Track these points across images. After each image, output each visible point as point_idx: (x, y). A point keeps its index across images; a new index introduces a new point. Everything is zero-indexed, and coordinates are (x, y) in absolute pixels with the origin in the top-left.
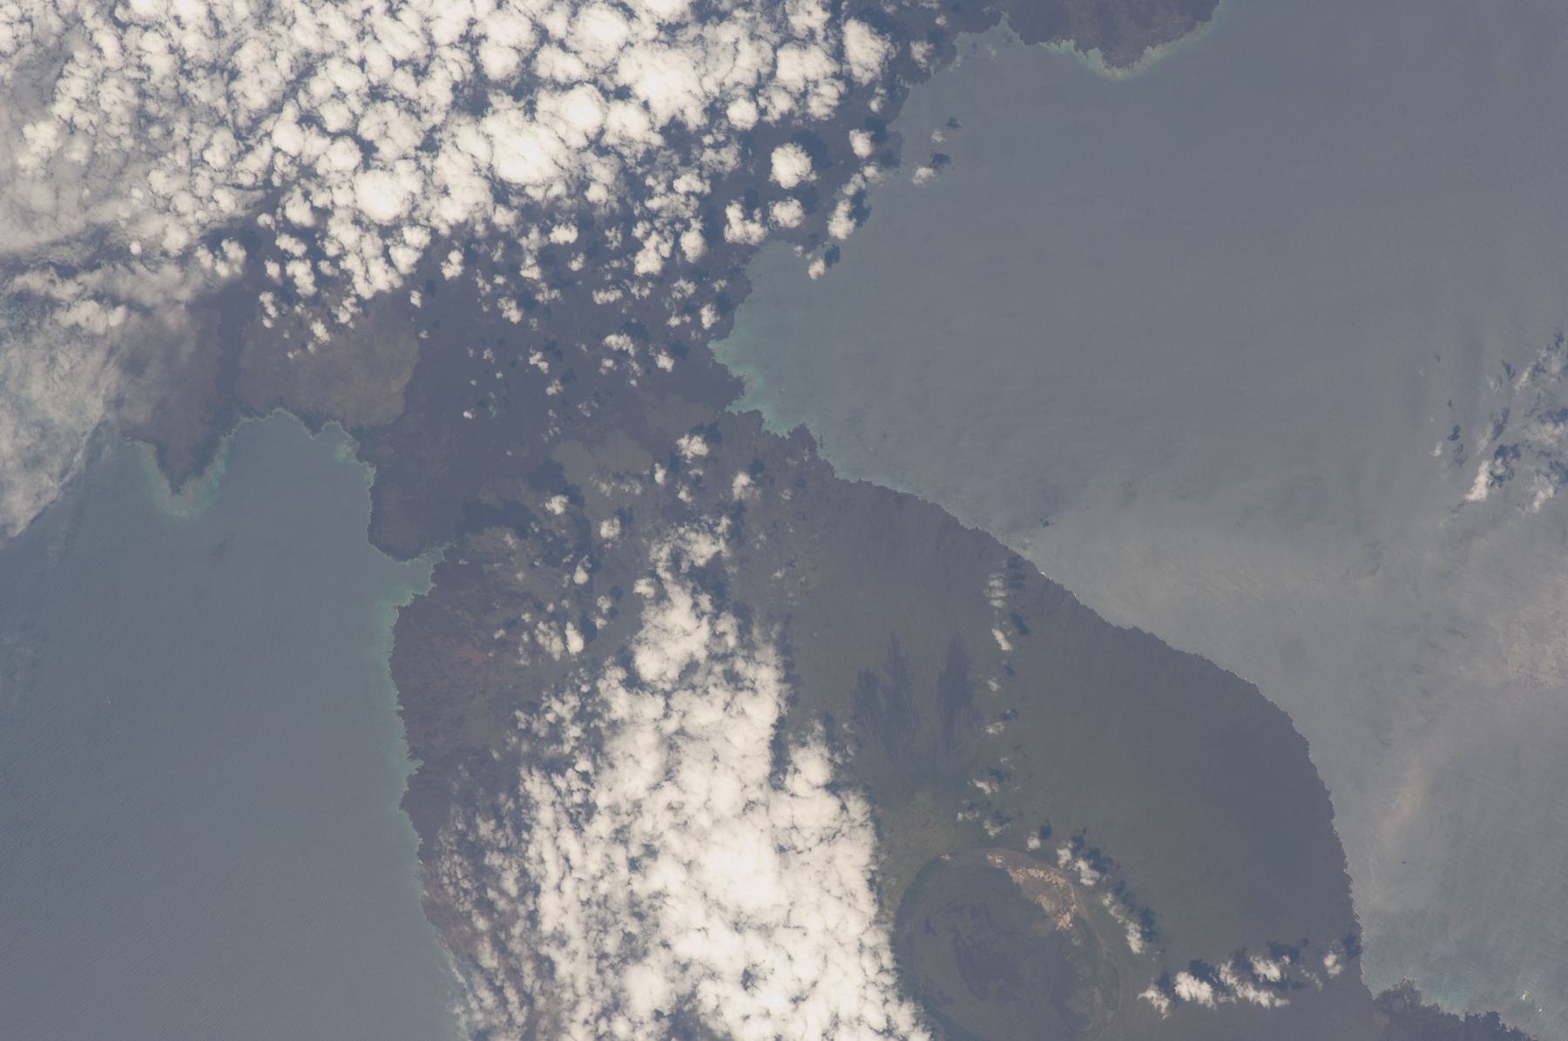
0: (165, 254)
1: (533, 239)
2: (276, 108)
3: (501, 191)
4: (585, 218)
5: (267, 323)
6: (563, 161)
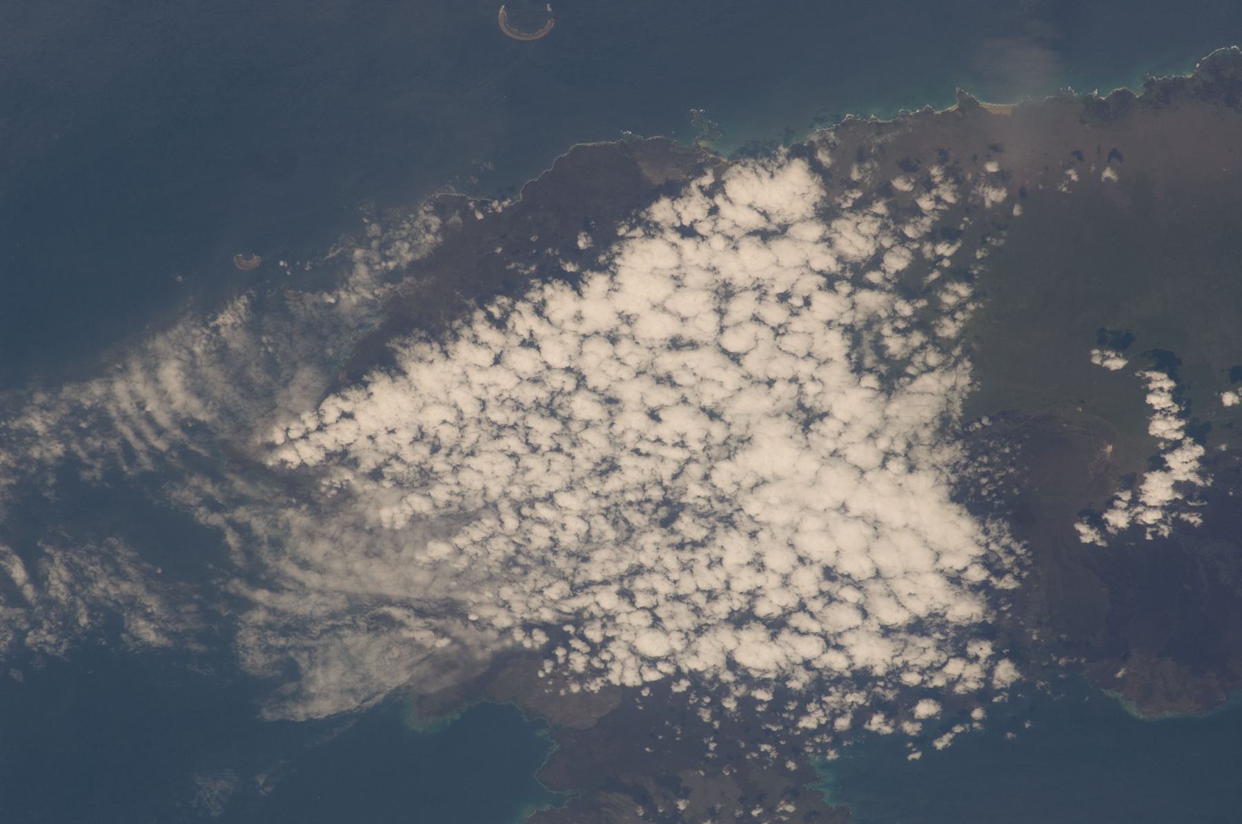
0: (492, 625)
1: (741, 691)
2: (605, 583)
3: (732, 664)
4: (782, 694)
5: (541, 674)
6: (783, 665)
